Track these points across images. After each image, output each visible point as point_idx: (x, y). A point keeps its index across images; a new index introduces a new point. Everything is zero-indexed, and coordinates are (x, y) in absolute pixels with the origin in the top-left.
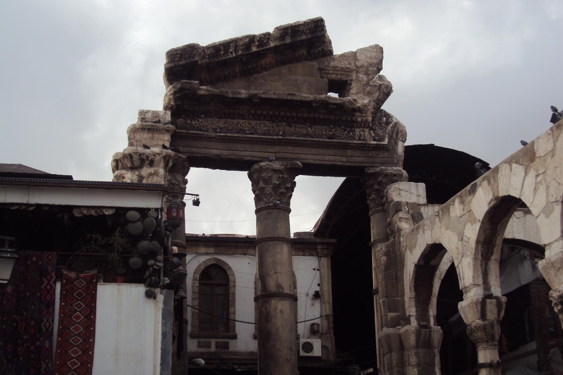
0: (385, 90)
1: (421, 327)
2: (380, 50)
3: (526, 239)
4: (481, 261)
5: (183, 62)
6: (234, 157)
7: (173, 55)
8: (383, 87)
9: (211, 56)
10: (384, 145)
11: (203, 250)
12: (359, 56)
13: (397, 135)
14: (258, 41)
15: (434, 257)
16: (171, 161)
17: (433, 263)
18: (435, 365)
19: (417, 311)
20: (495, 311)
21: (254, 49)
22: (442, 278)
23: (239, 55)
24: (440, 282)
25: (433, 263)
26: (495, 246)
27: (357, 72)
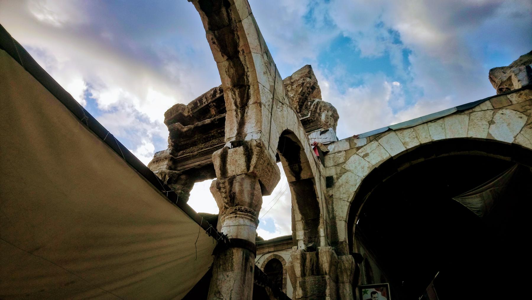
0: (308, 85)
1: (309, 249)
2: (310, 66)
3: (448, 137)
4: (236, 111)
5: (173, 116)
6: (209, 163)
7: (168, 114)
8: (305, 84)
9: (193, 109)
10: (307, 118)
11: (267, 250)
12: (293, 77)
13: (320, 109)
14: (220, 90)
15: (301, 169)
16: (167, 176)
17: (304, 176)
18: (325, 295)
19: (305, 234)
20: (242, 161)
21: (218, 96)
22: (350, 200)
23: (210, 103)
24: (348, 204)
25: (304, 176)
26: (249, 86)
27: (292, 85)
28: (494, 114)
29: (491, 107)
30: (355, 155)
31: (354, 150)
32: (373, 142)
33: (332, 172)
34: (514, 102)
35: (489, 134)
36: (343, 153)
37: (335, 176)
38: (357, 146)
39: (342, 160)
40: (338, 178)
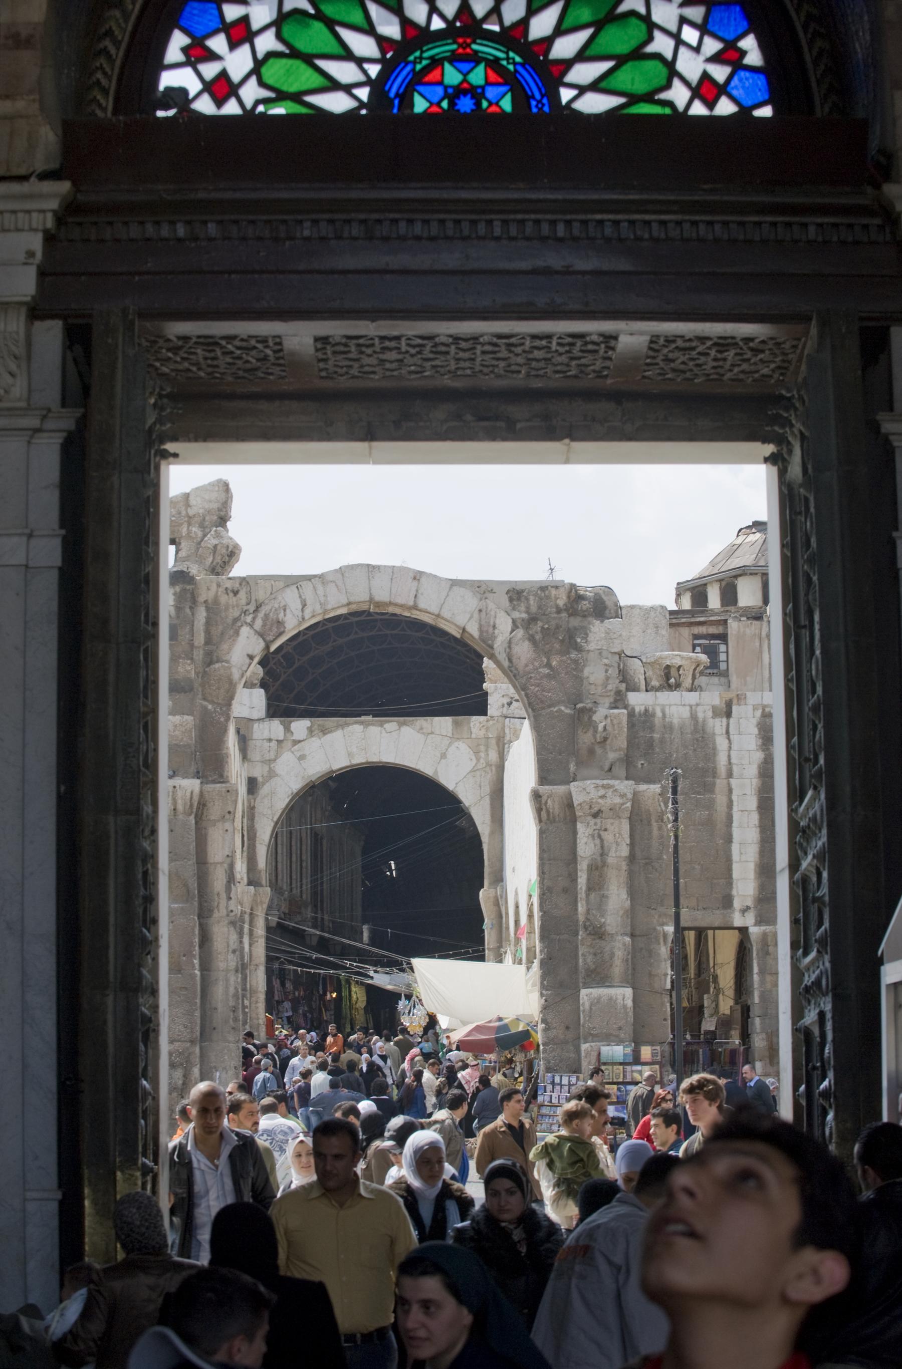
0: (224, 551)
8: (219, 547)
12: (192, 501)
28: (450, 745)
29: (450, 735)
30: (289, 753)
31: (289, 743)
32: (314, 739)
33: (258, 772)
34: (473, 736)
35: (436, 772)
36: (274, 744)
37: (260, 779)
38: (293, 738)
39: (272, 755)
40: (264, 784)
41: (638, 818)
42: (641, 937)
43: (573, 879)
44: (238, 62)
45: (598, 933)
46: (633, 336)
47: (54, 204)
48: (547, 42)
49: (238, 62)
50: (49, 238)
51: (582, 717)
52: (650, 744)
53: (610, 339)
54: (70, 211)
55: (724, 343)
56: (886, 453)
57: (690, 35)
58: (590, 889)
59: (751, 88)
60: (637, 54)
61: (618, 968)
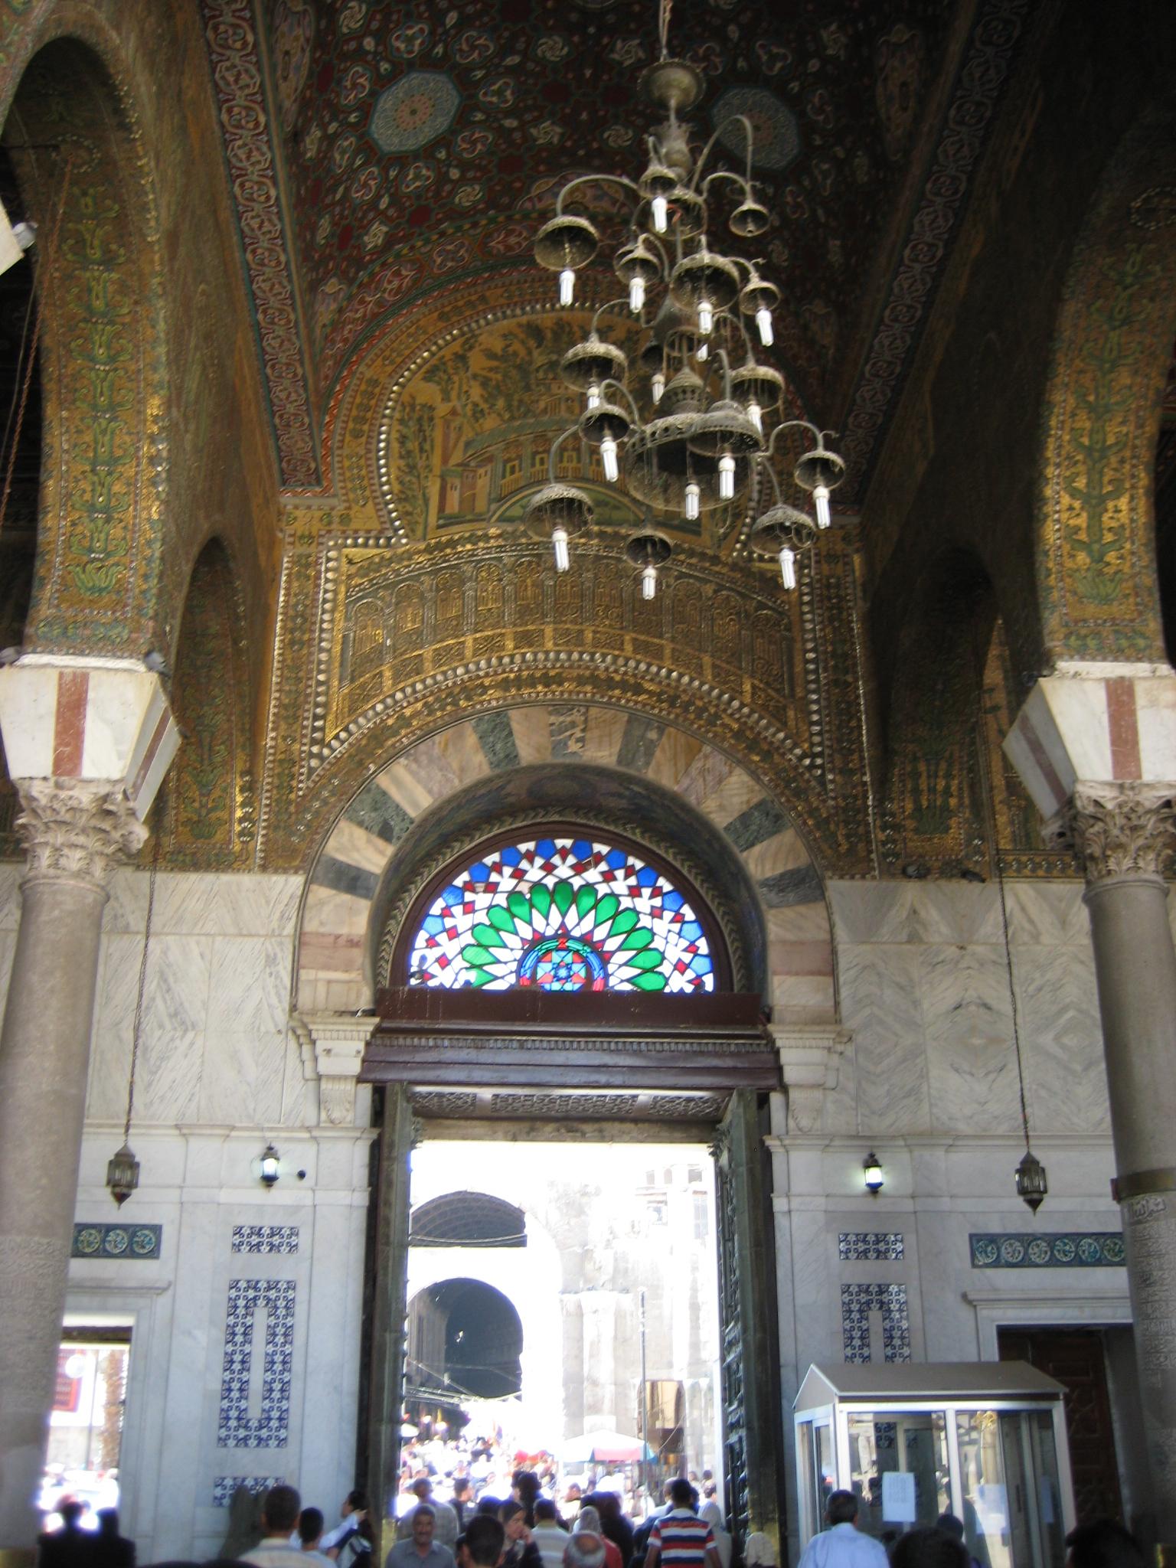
41: (619, 1316)
42: (620, 1385)
43: (581, 1349)
44: (450, 948)
45: (595, 1383)
46: (644, 1095)
47: (371, 1028)
48: (603, 941)
49: (450, 948)
50: (368, 1044)
51: (586, 1254)
52: (626, 1270)
53: (635, 1097)
54: (378, 1031)
55: (689, 1100)
56: (767, 1156)
57: (673, 938)
58: (591, 1356)
59: (702, 965)
60: (646, 948)
61: (607, 1405)
